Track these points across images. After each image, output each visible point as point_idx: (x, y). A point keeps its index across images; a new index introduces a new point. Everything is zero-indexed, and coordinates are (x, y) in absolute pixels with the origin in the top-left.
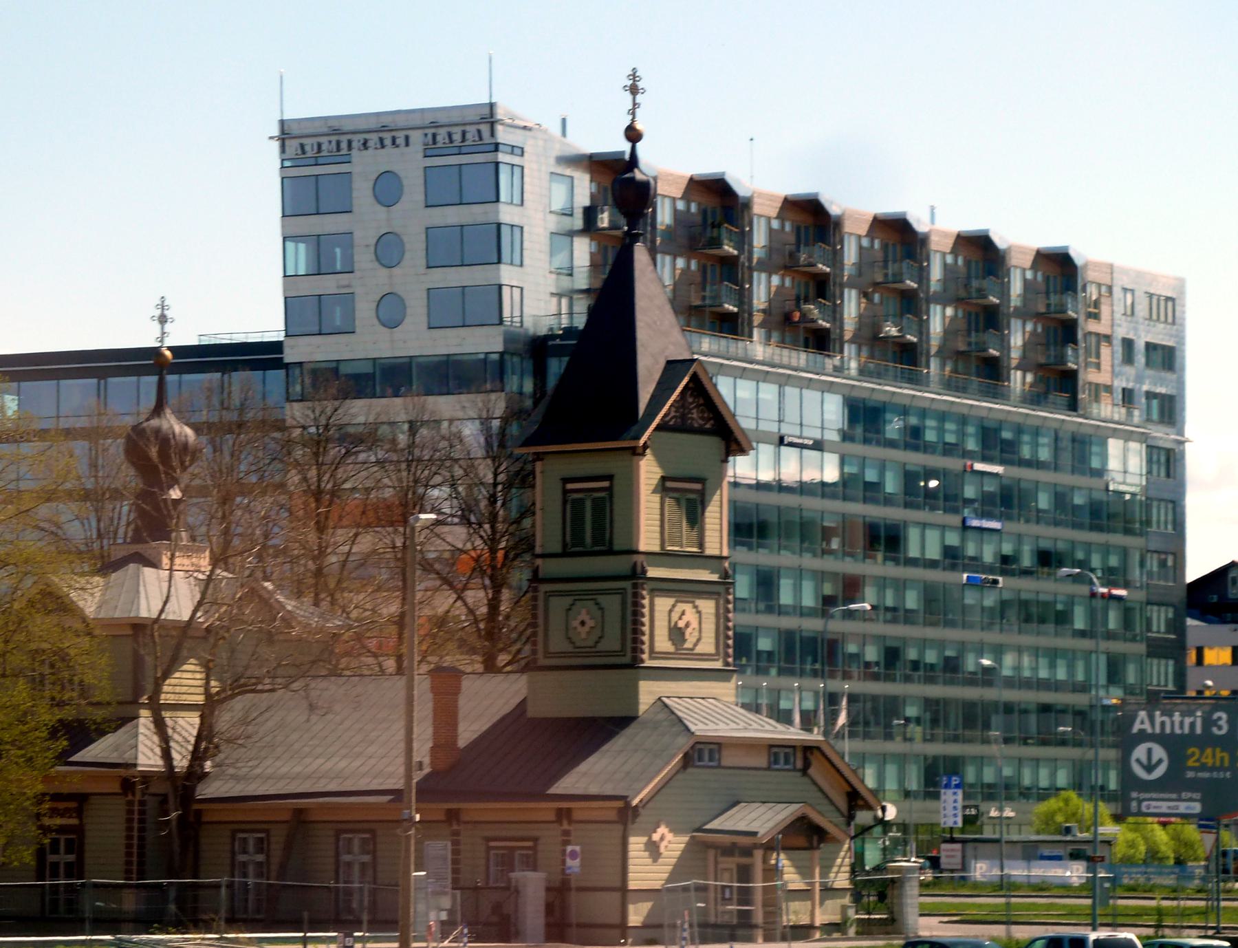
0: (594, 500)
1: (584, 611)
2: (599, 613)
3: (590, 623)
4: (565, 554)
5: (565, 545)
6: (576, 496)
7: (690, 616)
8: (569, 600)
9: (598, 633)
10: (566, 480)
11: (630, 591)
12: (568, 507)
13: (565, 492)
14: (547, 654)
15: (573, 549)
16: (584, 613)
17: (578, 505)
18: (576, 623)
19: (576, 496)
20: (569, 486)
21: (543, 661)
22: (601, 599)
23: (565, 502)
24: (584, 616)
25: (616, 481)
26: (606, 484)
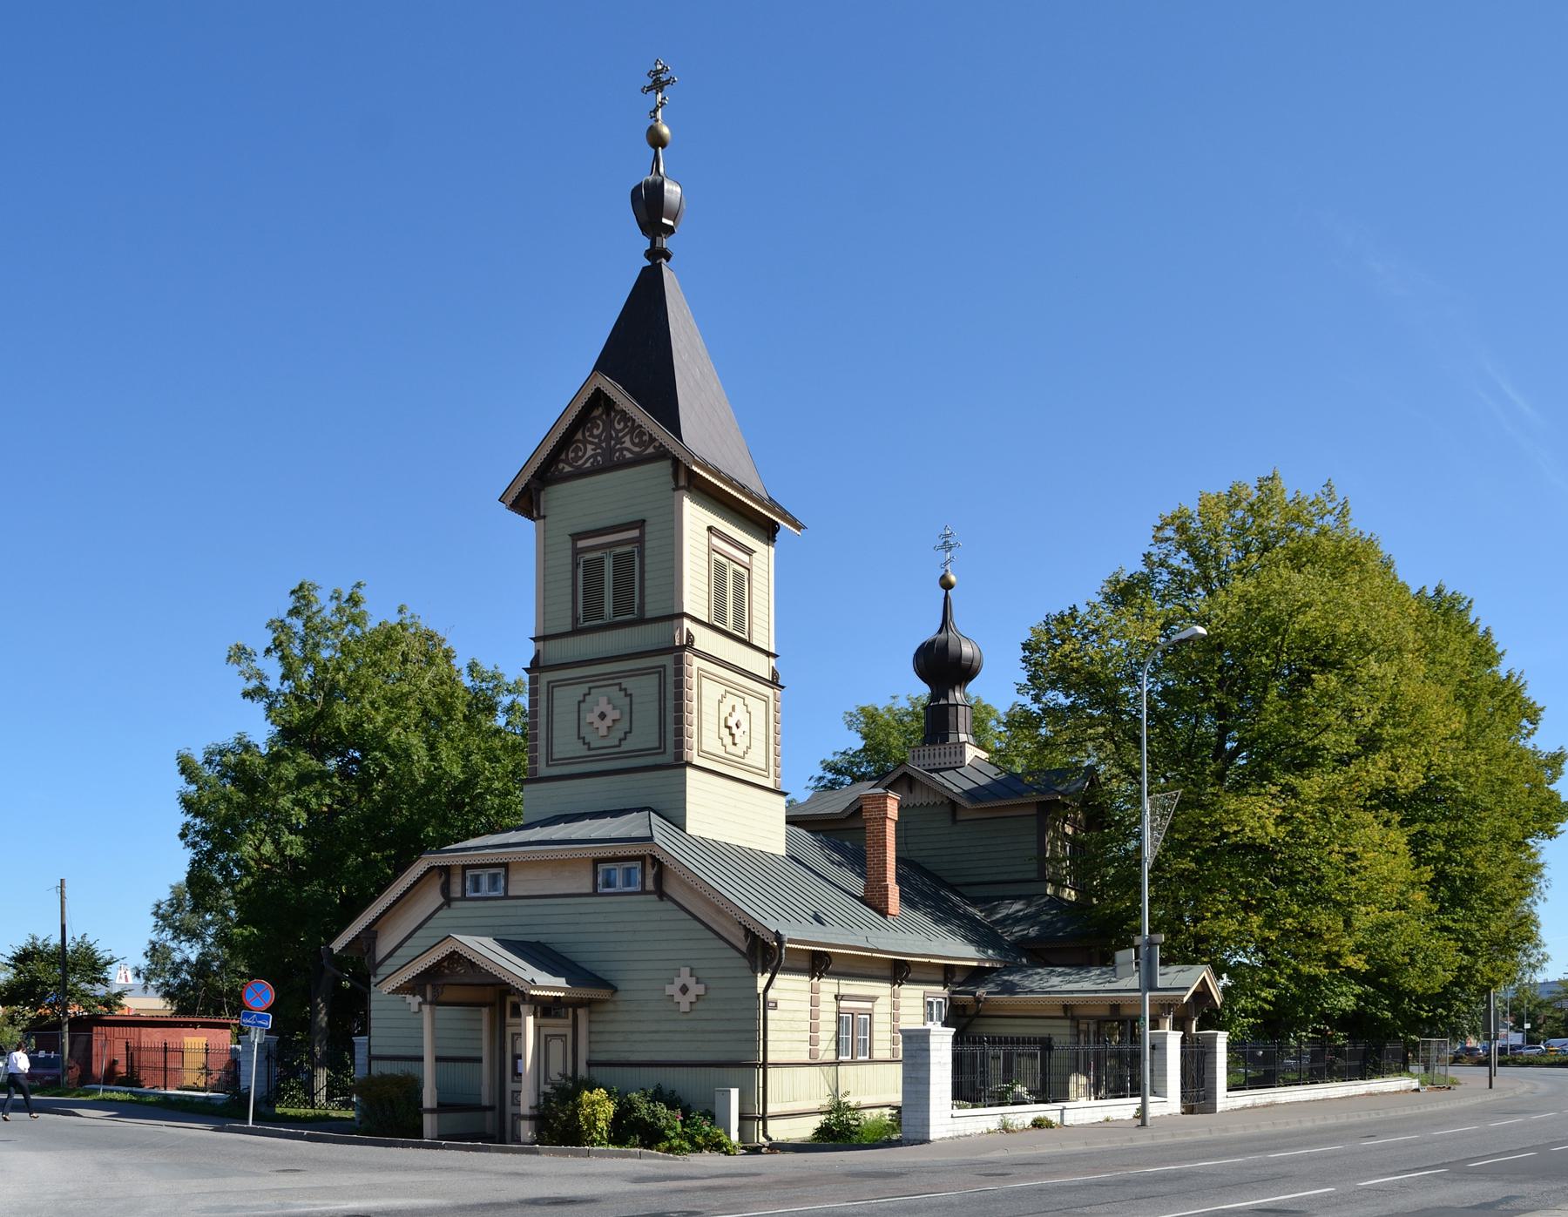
0: (617, 558)
1: (603, 700)
2: (585, 731)
3: (613, 714)
4: (576, 632)
5: (575, 619)
6: (588, 556)
7: (740, 714)
8: (584, 688)
9: (624, 725)
10: (576, 537)
11: (670, 671)
12: (580, 571)
13: (576, 552)
14: (551, 760)
15: (587, 624)
16: (601, 701)
17: (594, 569)
18: (592, 717)
19: (588, 556)
20: (581, 544)
21: (543, 770)
22: (626, 683)
23: (575, 565)
24: (603, 706)
25: (648, 529)
26: (635, 533)
